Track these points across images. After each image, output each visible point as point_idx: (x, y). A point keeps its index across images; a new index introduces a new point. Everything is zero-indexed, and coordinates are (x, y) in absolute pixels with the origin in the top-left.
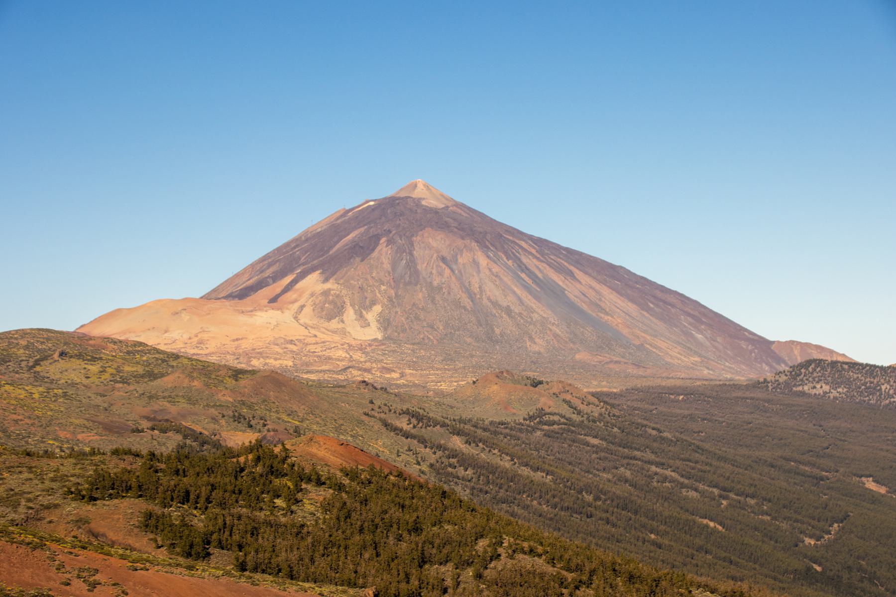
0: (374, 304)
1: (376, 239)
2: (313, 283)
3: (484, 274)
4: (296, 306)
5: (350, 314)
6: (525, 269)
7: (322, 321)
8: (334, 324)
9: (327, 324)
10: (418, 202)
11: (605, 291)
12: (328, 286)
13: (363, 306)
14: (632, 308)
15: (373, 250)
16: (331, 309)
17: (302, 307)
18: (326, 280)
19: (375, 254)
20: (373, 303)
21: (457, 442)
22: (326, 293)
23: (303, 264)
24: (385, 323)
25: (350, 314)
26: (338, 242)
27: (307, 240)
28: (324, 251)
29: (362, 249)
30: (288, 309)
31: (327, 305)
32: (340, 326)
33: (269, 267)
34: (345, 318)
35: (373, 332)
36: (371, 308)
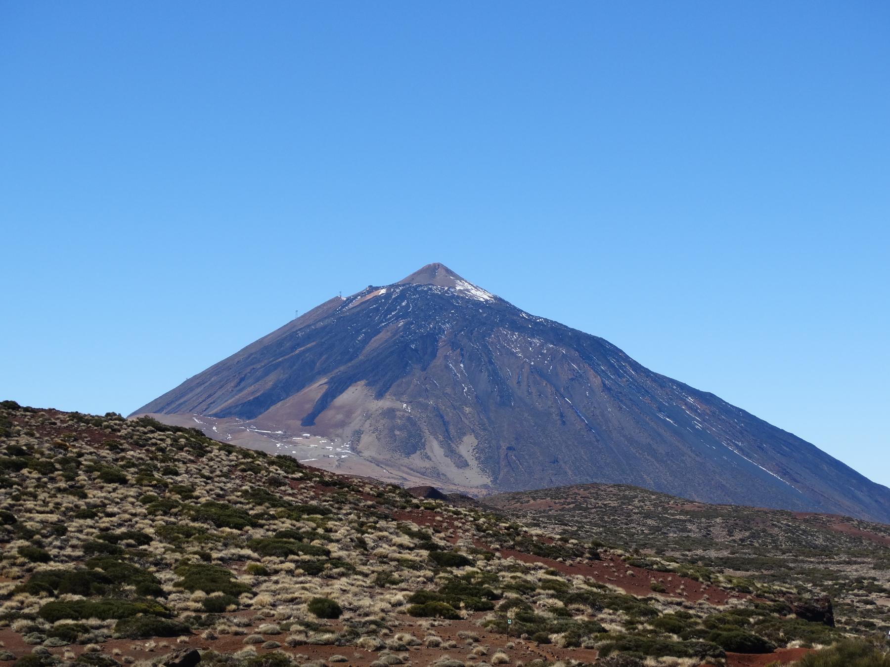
0: (464, 434)
4: (348, 431)
5: (435, 448)
7: (397, 455)
8: (416, 460)
9: (406, 461)
12: (386, 403)
15: (434, 355)
17: (358, 434)
18: (380, 395)
19: (438, 361)
20: (462, 434)
22: (390, 413)
23: (323, 372)
26: (365, 342)
27: (309, 338)
30: (338, 436)
31: (397, 433)
32: (427, 464)
33: (267, 373)
34: (429, 454)
36: (460, 438)
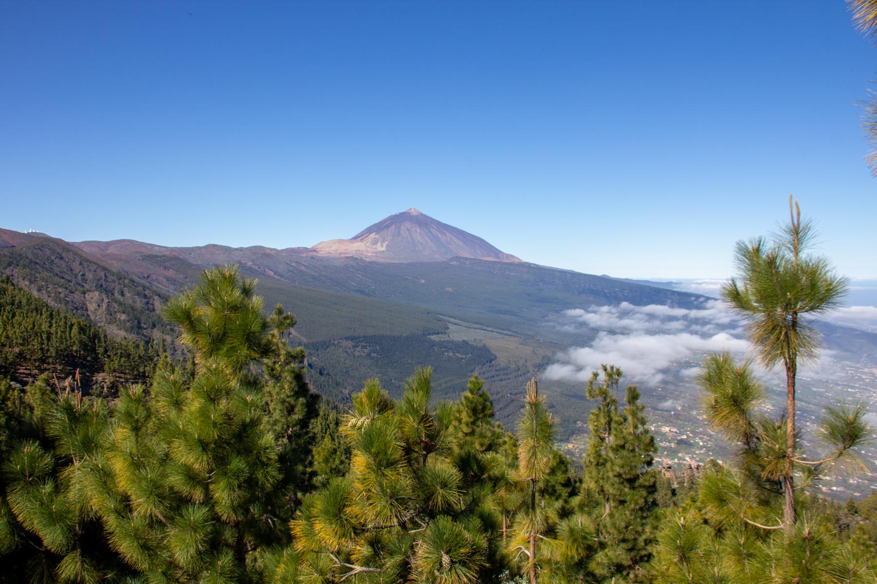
1: (391, 224)
2: (373, 235)
3: (418, 234)
5: (379, 244)
6: (431, 233)
10: (409, 213)
11: (454, 239)
13: (384, 242)
14: (460, 243)
16: (375, 242)
21: (303, 268)
24: (388, 246)
25: (379, 244)
28: (378, 228)
29: (387, 227)
35: (384, 249)
